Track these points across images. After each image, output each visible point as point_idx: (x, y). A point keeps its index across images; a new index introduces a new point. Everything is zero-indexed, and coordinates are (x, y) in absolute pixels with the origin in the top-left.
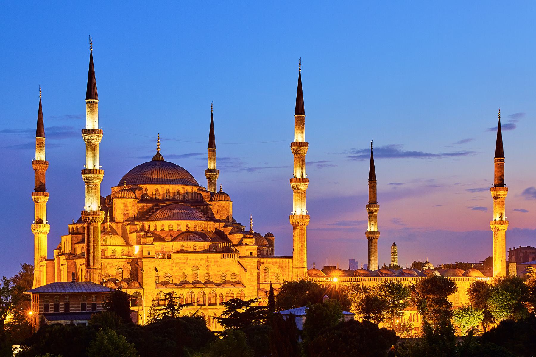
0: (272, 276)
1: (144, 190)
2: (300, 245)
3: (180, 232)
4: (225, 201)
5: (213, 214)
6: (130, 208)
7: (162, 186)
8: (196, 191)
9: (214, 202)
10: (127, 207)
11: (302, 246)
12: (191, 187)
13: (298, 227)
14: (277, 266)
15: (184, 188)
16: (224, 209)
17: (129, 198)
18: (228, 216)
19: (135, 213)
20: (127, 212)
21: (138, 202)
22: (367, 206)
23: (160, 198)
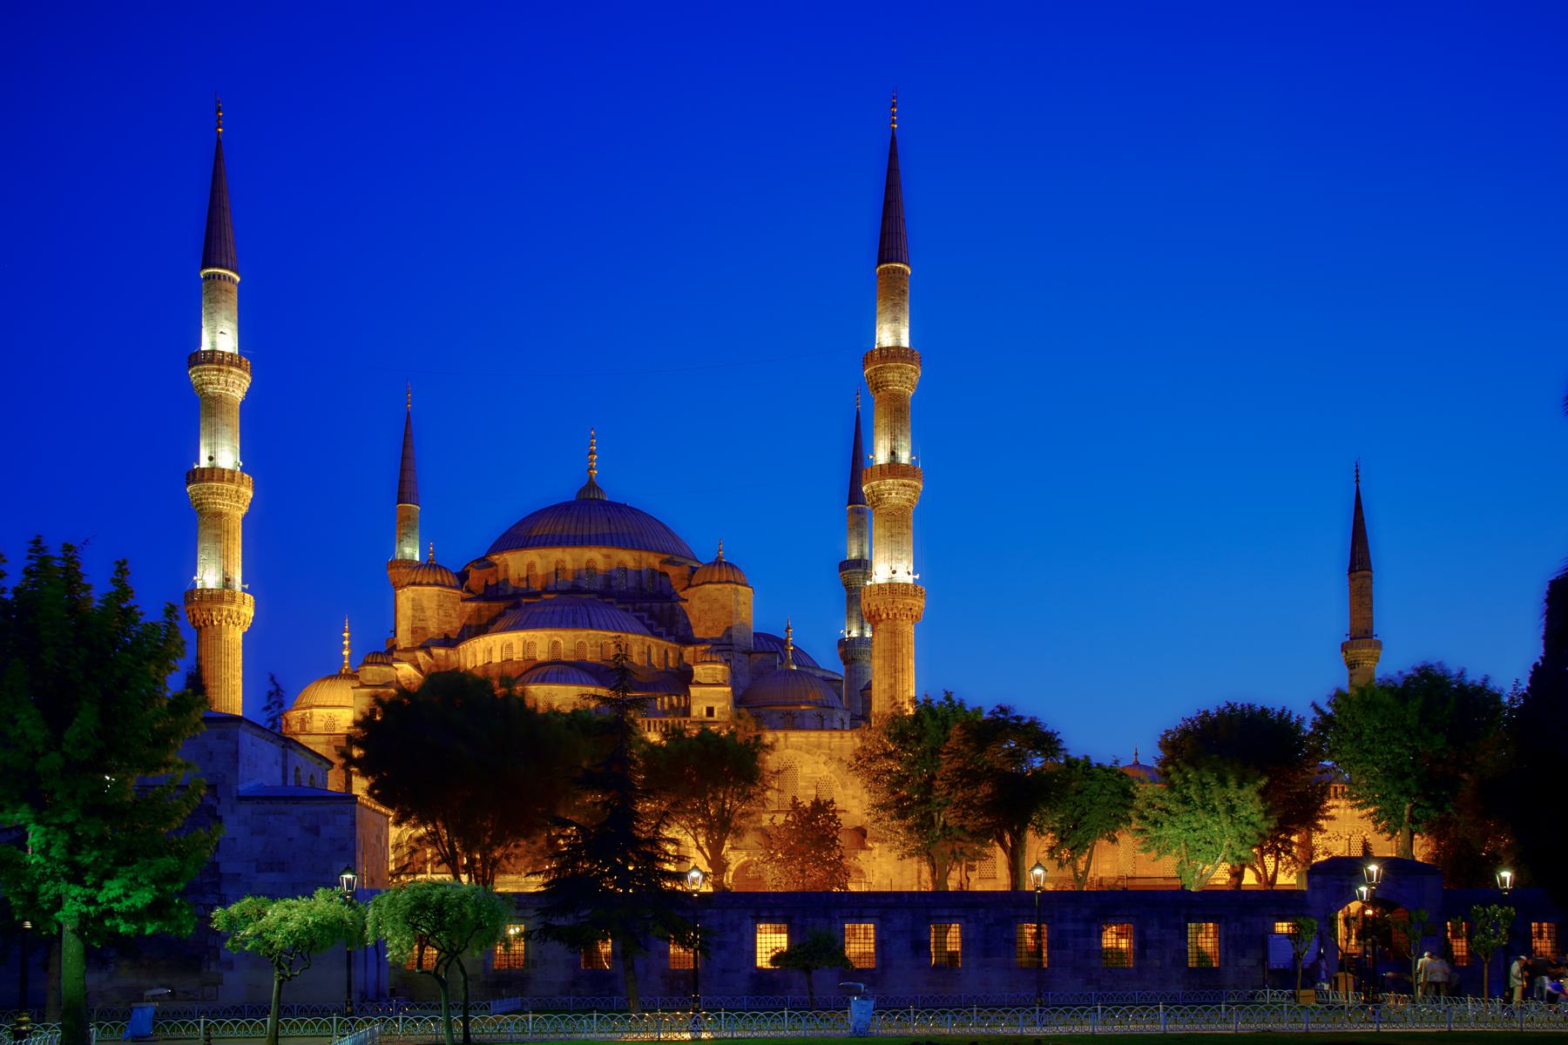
0: (807, 788)
1: (501, 569)
2: (884, 686)
3: (532, 664)
4: (719, 582)
5: (689, 626)
6: (429, 613)
7: (544, 551)
8: (657, 566)
9: (691, 590)
10: (423, 610)
11: (892, 686)
12: (636, 554)
13: (881, 626)
14: (824, 758)
15: (608, 557)
16: (716, 606)
17: (428, 584)
18: (729, 628)
19: (447, 628)
20: (420, 624)
21: (463, 600)
22: (1344, 647)
23: (537, 586)
